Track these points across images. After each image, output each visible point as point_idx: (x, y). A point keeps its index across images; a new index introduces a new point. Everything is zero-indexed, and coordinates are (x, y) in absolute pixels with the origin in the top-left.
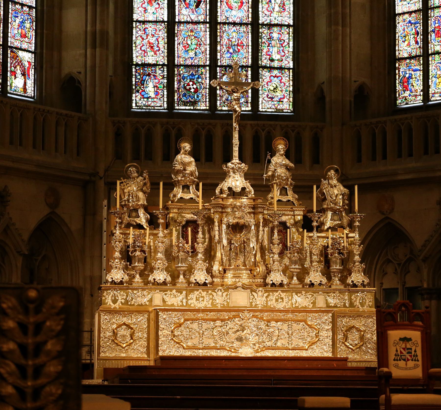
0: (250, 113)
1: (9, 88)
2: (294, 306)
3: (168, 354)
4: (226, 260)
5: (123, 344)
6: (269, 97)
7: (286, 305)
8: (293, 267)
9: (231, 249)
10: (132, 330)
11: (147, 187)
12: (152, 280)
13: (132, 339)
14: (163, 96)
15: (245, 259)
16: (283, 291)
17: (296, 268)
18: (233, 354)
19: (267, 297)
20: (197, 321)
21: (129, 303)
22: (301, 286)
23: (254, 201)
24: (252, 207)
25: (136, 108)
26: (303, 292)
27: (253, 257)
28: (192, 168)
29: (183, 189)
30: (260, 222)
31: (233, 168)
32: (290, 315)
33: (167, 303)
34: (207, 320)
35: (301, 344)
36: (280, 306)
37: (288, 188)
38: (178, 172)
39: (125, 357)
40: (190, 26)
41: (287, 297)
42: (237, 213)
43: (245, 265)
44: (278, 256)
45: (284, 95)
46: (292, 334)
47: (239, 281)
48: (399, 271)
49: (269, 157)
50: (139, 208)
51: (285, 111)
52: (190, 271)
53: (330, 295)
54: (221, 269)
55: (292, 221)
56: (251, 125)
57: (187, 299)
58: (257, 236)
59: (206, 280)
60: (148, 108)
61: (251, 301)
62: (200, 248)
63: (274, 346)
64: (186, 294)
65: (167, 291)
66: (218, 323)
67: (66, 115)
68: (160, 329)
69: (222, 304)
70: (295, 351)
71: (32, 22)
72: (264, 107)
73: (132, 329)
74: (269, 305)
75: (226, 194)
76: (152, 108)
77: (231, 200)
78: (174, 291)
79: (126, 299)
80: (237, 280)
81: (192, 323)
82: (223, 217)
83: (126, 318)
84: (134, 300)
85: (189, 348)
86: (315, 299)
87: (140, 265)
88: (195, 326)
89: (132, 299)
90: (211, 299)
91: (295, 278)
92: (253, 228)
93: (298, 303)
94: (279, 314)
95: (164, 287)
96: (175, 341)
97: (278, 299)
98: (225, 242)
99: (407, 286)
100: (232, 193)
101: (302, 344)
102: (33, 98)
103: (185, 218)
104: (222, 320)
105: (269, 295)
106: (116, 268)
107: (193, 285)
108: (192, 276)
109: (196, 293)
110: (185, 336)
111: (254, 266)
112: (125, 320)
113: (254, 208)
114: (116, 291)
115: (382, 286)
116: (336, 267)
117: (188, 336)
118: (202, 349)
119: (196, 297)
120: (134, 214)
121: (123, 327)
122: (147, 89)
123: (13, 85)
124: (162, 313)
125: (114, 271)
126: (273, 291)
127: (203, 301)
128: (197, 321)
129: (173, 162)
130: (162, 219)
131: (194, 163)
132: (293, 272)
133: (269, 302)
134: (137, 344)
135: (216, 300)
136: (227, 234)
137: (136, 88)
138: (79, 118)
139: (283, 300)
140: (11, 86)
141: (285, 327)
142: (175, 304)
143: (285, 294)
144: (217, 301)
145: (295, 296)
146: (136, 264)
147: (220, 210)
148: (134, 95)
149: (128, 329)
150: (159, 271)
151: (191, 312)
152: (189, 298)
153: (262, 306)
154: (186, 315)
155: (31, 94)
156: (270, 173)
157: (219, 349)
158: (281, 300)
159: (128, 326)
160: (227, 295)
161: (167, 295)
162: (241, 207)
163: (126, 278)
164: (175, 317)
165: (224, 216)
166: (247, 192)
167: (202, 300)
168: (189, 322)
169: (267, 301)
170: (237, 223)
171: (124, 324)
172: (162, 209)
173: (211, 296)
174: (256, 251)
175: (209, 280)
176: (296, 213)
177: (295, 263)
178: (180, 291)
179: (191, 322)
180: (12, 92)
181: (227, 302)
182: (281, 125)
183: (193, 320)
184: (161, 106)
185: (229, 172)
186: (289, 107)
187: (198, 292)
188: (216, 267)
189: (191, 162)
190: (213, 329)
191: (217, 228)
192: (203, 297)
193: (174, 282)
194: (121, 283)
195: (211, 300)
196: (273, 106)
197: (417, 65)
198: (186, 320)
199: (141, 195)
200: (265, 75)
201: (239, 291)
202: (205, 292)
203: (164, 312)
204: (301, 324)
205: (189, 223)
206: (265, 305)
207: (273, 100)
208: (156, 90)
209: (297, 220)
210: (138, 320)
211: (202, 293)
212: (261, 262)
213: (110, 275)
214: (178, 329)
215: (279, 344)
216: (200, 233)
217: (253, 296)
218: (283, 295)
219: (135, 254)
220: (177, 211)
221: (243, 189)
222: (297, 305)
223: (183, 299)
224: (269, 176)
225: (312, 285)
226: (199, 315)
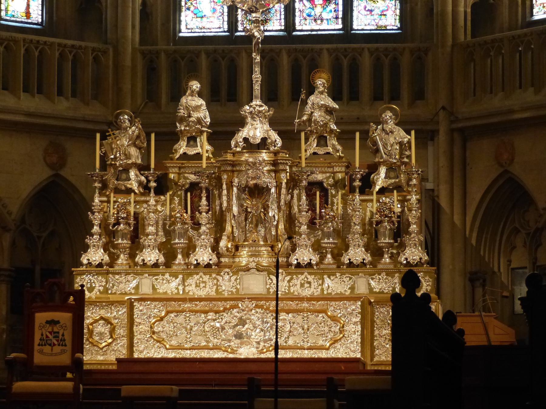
0: (341, 32)
1: (3, 14)
2: (325, 293)
3: (146, 356)
4: (239, 234)
5: (101, 344)
6: (367, 9)
7: (315, 291)
8: (326, 241)
9: (246, 219)
10: (112, 326)
11: (141, 141)
12: (140, 261)
13: (111, 337)
14: (223, 14)
15: (265, 231)
16: (310, 274)
18: (231, 356)
19: (289, 281)
20: (183, 313)
21: (110, 292)
22: (335, 266)
23: (275, 155)
24: (271, 164)
25: (187, 31)
26: (338, 275)
27: (274, 228)
29: (188, 142)
30: (282, 183)
31: (251, 113)
32: (305, 305)
33: (158, 291)
34: (196, 312)
35: (321, 343)
36: (307, 292)
37: (328, 137)
38: (182, 120)
39: (102, 361)
41: (315, 281)
42: (250, 172)
43: (265, 240)
44: (306, 227)
45: (388, 6)
46: (308, 330)
47: (254, 261)
48: (528, 243)
49: (303, 96)
50: (131, 168)
51: (388, 28)
53: (374, 277)
54: (229, 246)
55: (331, 181)
56: (328, 50)
57: (184, 285)
58: (279, 202)
59: (210, 260)
60: (203, 31)
61: (268, 286)
62: (204, 218)
63: (285, 344)
64: (183, 278)
65: (158, 275)
66: (211, 315)
67: (73, 46)
68: (136, 324)
69: (230, 291)
70: (312, 352)
72: (360, 24)
73: (112, 324)
74: (292, 291)
75: (240, 147)
76: (209, 31)
77: (247, 155)
78: (167, 276)
79: (105, 287)
80: (251, 260)
81: (178, 315)
82: (233, 177)
83: (104, 311)
84: (115, 288)
85: (173, 348)
86: (354, 283)
88: (181, 319)
89: (113, 285)
90: (215, 285)
91: (329, 256)
92: (273, 190)
93: (330, 288)
94: (291, 303)
95: (155, 270)
96: (154, 340)
97: (304, 283)
98: (235, 209)
99: (538, 264)
101: (321, 342)
102: (41, 24)
103: (189, 179)
104: (216, 312)
105: (292, 279)
106: (94, 246)
107: (192, 267)
108: (192, 255)
109: (196, 277)
110: (168, 332)
111: (276, 240)
112: (103, 313)
114: (93, 276)
115: (510, 265)
116: (385, 240)
117: (171, 333)
118: (190, 349)
119: (196, 283)
120: (124, 176)
121: (100, 322)
122: (200, 5)
123: (10, 8)
124: (138, 303)
125: (91, 251)
126: (297, 274)
127: (205, 287)
128: (184, 314)
129: (178, 106)
130: (155, 181)
131: (204, 107)
132: (326, 248)
133: (291, 288)
134: (118, 344)
135: (221, 286)
136: (239, 198)
137: (186, 4)
138: (94, 50)
139: (310, 285)
140: (7, 10)
141: (299, 319)
142: (169, 292)
143: (313, 276)
144: (224, 288)
145: (327, 281)
146: (120, 241)
147: (229, 168)
148: (183, 14)
149: (107, 325)
150: (149, 250)
151: (175, 302)
152: (186, 285)
153: (284, 293)
154: (170, 306)
155: (37, 19)
156: (305, 118)
157: (211, 349)
158: (308, 285)
159: (107, 321)
160: (236, 280)
161: (159, 280)
162: (254, 164)
163: (106, 258)
164: (158, 310)
165: (235, 176)
166: (269, 143)
167: (203, 287)
168: (172, 315)
169: (289, 287)
170: (256, 185)
171: (102, 318)
172: (155, 169)
173: (215, 281)
174: (278, 222)
175: (215, 259)
176: (336, 169)
177: (328, 236)
178: (175, 275)
179: (176, 314)
180: (8, 18)
181: (236, 288)
182: (369, 49)
184: (220, 28)
185: (247, 117)
186: (395, 22)
187: (198, 276)
188: (223, 244)
189: (197, 108)
190: (205, 323)
191: (225, 192)
192: (204, 282)
193: (168, 264)
194: (100, 265)
195: (216, 286)
196: (373, 21)
198: (168, 313)
199: (133, 151)
201: (253, 273)
202: (208, 276)
203: (140, 302)
204: (321, 315)
205: (194, 187)
206: (287, 291)
207: (373, 13)
208: (213, 6)
209: (336, 179)
210: (120, 313)
211: (204, 276)
212: (285, 235)
213: (86, 256)
214: (159, 324)
215: (291, 342)
216: (204, 199)
217: (271, 280)
218: (311, 278)
219: (117, 228)
220: (177, 171)
221: (264, 140)
222: (329, 291)
223: (179, 285)
224: (304, 121)
225: (351, 264)
226: (186, 306)
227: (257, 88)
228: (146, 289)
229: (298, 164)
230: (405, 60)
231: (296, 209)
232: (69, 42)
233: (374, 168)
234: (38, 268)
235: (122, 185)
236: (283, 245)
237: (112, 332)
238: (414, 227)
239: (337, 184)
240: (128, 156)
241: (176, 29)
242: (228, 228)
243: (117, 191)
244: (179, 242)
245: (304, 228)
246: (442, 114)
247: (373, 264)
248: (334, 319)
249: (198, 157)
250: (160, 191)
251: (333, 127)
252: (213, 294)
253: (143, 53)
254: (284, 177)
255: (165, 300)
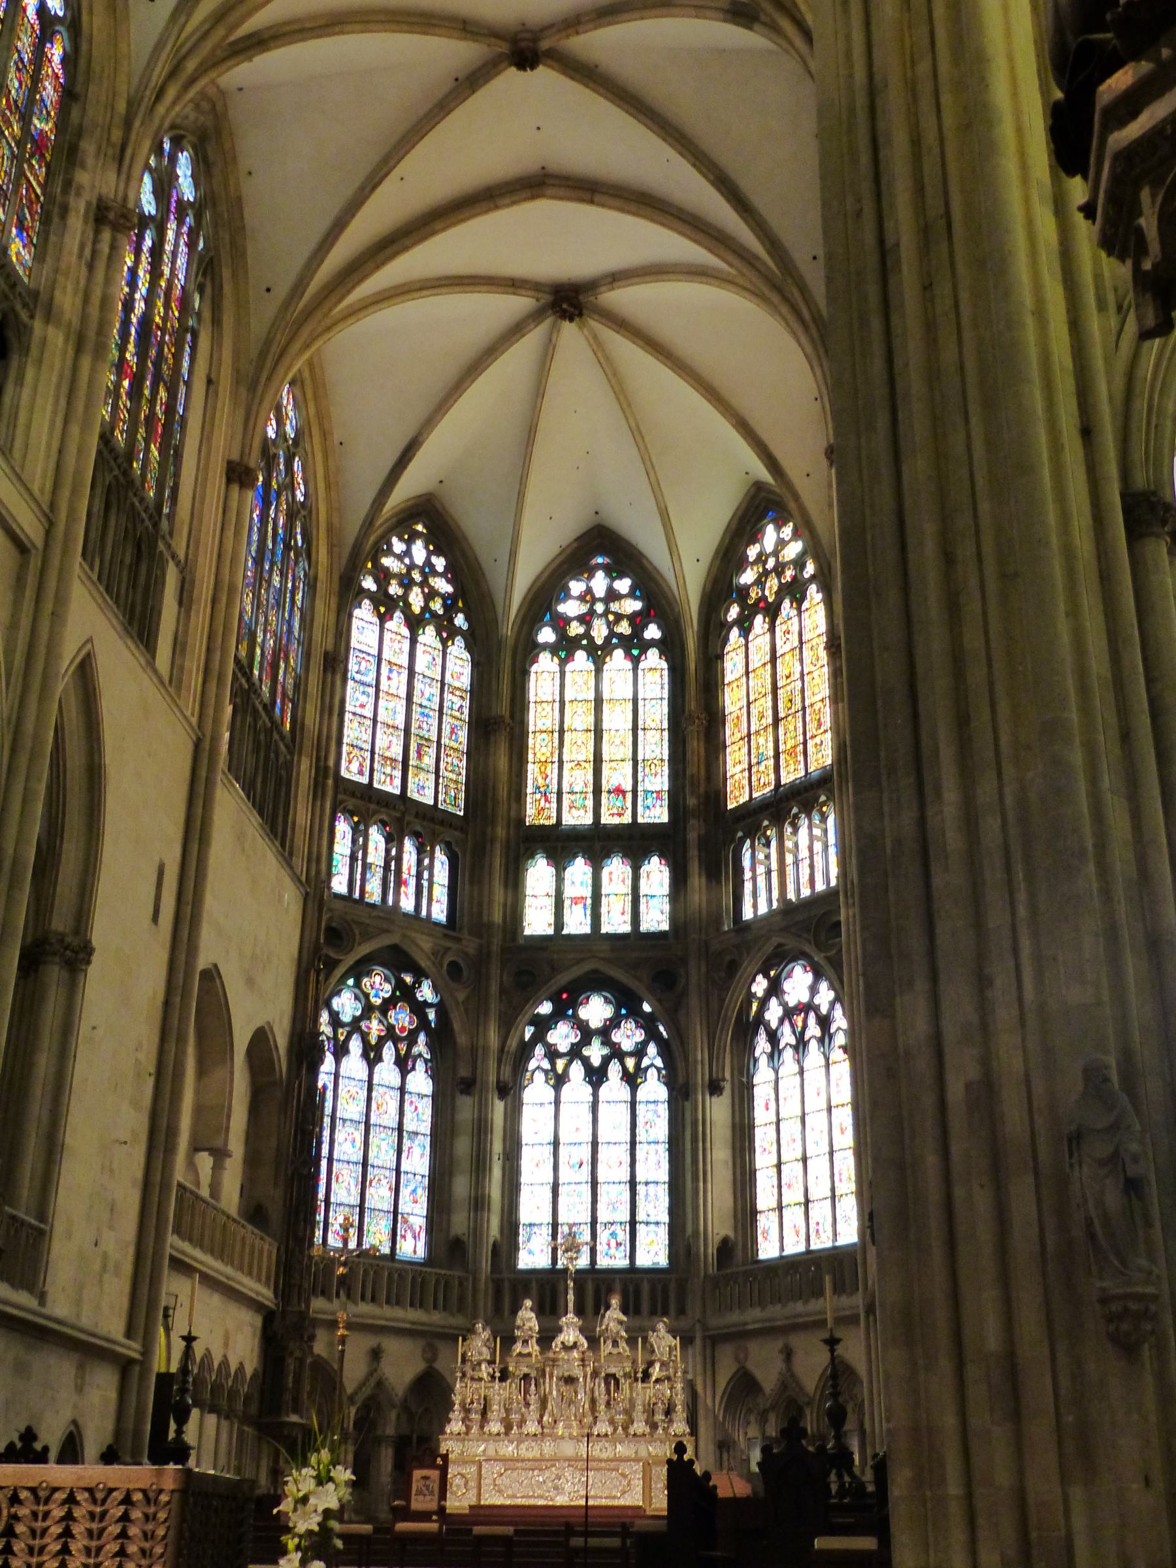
17: (620, 1418)
18: (551, 1503)
28: (534, 1324)
32: (603, 1464)
35: (614, 1493)
36: (604, 1455)
38: (519, 1328)
40: (573, 1187)
43: (575, 1416)
52: (522, 1423)
55: (621, 1373)
62: (533, 1399)
71: (424, 1188)
85: (509, 1497)
87: (476, 1417)
88: (515, 1473)
98: (555, 1393)
100: (566, 1348)
104: (540, 1470)
113: (583, 1360)
116: (659, 1417)
136: (557, 1385)
145: (619, 1448)
159: (463, 1476)
163: (464, 1429)
164: (498, 1467)
170: (569, 1377)
175: (540, 1430)
183: (513, 1469)
188: (545, 1418)
189: (530, 1319)
193: (507, 1433)
197: (774, 1216)
199: (485, 1350)
200: (641, 1229)
205: (526, 1377)
218: (607, 1445)
221: (575, 1343)
227: (571, 1305)
228: (491, 1452)
229: (599, 1361)
230: (672, 1287)
231: (597, 1393)
232: (443, 1272)
233: (651, 1364)
234: (415, 1436)
235: (476, 1375)
236: (588, 1420)
237: (466, 1485)
238: (679, 1408)
239: (626, 1376)
240: (480, 1354)
241: (515, 1264)
242: (549, 1407)
243: (472, 1379)
244: (515, 1417)
245: (603, 1407)
246: (698, 1326)
247: (651, 1434)
248: (624, 1476)
249: (529, 1355)
250: (503, 1379)
251: (624, 1334)
252: (538, 1456)
253: (493, 1280)
254: (589, 1370)
255: (503, 1460)
